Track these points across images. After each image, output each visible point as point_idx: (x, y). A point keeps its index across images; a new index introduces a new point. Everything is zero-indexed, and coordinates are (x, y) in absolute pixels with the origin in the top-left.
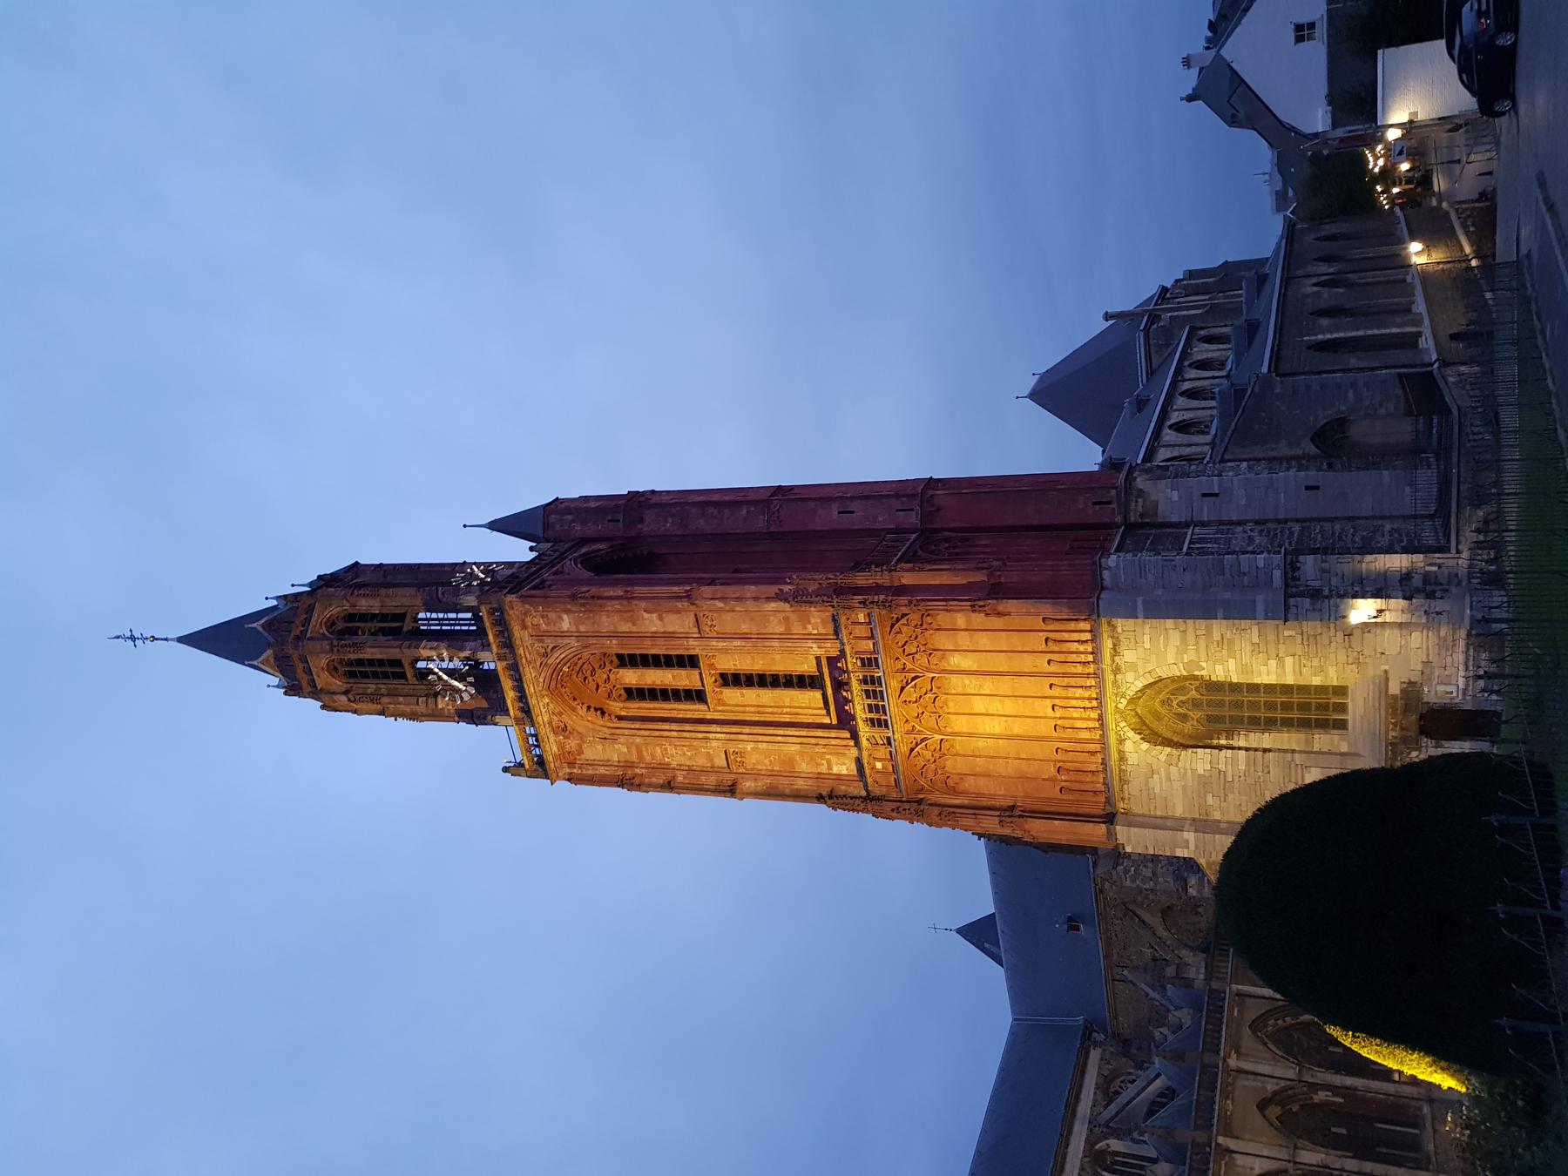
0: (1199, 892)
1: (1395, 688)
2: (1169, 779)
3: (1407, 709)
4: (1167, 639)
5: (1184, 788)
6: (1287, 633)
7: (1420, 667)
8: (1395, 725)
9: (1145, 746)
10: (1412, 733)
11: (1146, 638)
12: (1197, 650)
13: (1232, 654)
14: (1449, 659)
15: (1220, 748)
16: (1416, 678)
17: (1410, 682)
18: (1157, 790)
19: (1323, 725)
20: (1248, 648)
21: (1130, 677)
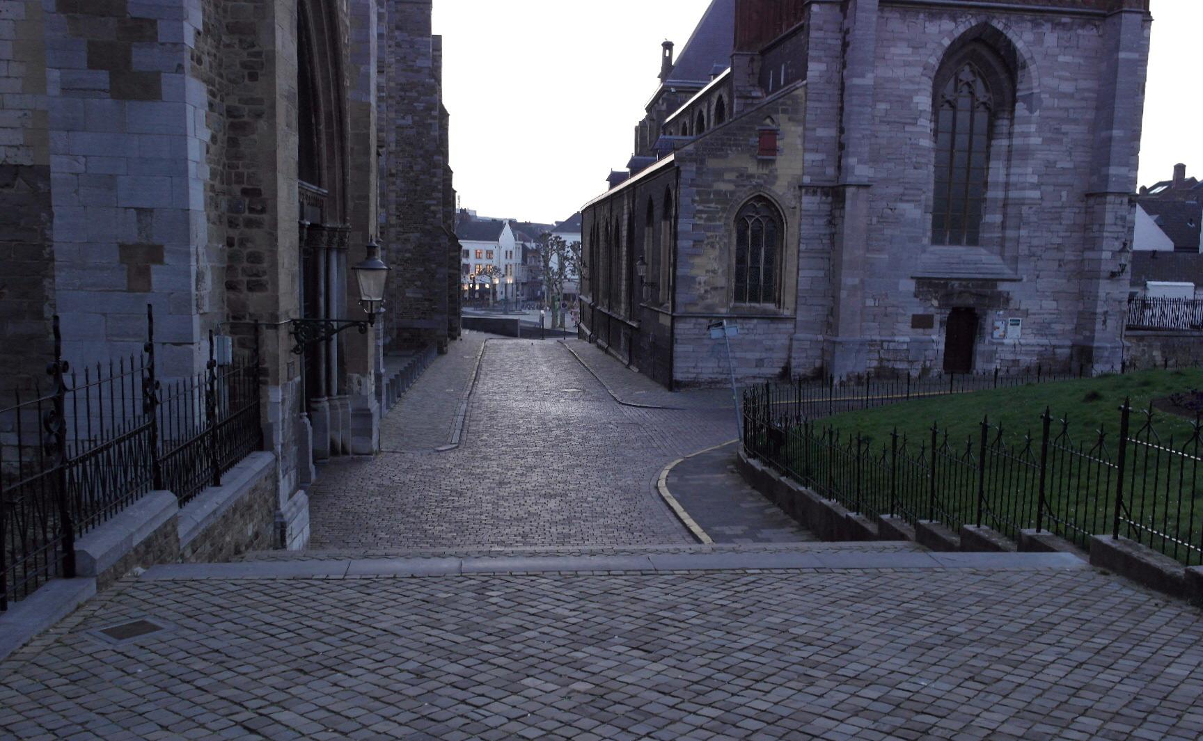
1: (1003, 287)
2: (907, 64)
3: (979, 296)
4: (1067, 79)
5: (896, 80)
6: (1064, 194)
7: (1023, 307)
8: (966, 286)
9: (947, 42)
10: (956, 302)
11: (1068, 59)
13: (1045, 140)
14: (1029, 331)
16: (1012, 305)
17: (1008, 300)
18: (893, 50)
20: (1051, 157)
21: (1028, 36)
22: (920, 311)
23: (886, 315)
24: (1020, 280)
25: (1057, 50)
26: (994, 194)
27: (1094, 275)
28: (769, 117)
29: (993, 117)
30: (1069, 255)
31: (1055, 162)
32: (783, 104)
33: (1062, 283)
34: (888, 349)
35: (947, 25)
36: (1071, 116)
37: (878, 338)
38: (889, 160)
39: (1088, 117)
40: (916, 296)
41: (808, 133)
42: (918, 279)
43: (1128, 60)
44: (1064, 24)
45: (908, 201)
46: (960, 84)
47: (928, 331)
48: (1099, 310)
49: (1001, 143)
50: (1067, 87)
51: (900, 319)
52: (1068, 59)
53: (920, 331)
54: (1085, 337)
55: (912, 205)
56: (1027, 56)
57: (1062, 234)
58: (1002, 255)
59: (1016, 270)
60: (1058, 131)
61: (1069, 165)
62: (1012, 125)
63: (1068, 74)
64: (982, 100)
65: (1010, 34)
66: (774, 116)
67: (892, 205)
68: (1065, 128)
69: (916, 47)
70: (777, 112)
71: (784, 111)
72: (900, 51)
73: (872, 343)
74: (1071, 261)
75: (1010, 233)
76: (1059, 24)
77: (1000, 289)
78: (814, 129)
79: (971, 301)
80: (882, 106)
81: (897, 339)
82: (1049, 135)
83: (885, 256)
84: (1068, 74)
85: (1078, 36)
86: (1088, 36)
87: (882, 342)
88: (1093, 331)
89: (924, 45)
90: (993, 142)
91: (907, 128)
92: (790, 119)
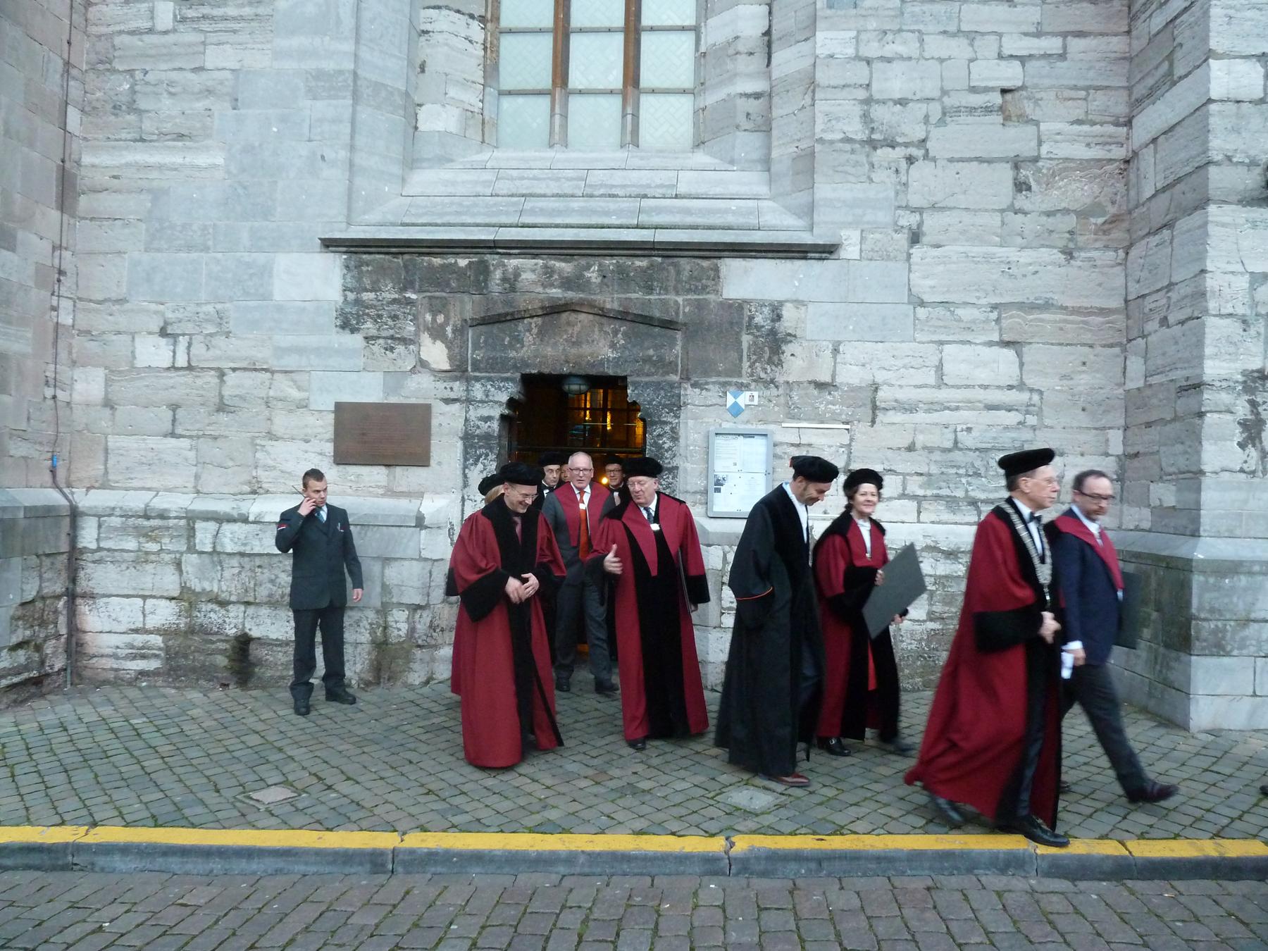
7: (850, 375)
16: (796, 364)
17: (774, 344)
22: (368, 389)
23: (222, 407)
24: (826, 251)
27: (1188, 196)
30: (1063, 135)
33: (1039, 269)
37: (176, 502)
40: (347, 324)
42: (354, 248)
47: (409, 477)
48: (1213, 369)
51: (282, 422)
53: (376, 475)
54: (1161, 512)
57: (1014, 45)
58: (766, 163)
59: (809, 210)
73: (149, 522)
74: (1068, 166)
75: (787, 60)
79: (602, 349)
83: (211, 157)
87: (192, 518)
88: (1193, 477)
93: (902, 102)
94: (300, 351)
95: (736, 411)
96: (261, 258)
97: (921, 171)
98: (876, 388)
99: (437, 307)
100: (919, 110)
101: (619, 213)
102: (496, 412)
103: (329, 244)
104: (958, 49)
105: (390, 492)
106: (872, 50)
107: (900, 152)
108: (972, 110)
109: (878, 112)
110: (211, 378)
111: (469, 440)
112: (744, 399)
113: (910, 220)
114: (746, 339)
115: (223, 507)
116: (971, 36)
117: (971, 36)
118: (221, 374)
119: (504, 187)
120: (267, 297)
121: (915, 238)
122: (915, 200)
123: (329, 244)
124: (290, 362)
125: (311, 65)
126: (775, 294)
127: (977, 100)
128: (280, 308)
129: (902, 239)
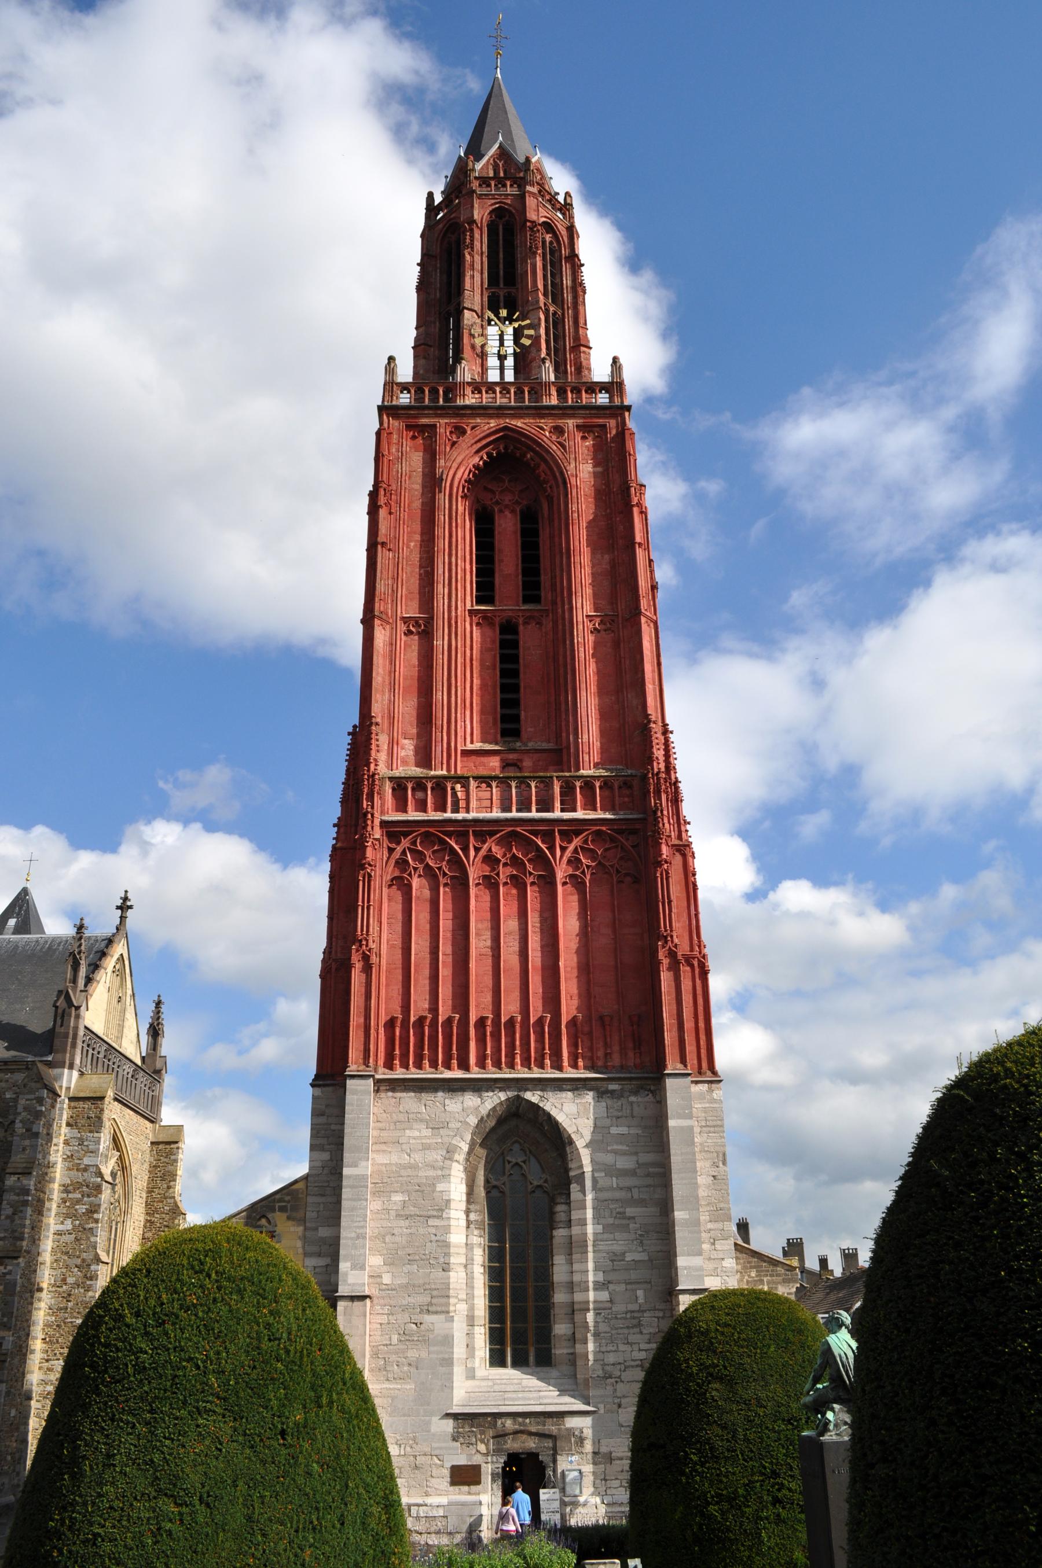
0: (12, 1189)
2: (426, 1147)
5: (414, 1167)
6: (640, 1293)
9: (473, 1121)
10: (513, 1445)
11: (624, 1130)
12: (611, 1189)
14: (617, 1483)
15: (468, 1212)
19: (496, 1337)
20: (617, 1248)
22: (462, 1460)
25: (608, 1122)
26: (559, 1297)
28: (264, 1216)
29: (553, 1202)
31: (624, 1254)
32: (281, 1200)
34: (418, 1518)
35: (470, 1100)
36: (636, 1196)
38: (410, 1262)
39: (657, 1196)
40: (455, 1439)
41: (308, 1234)
43: (682, 1128)
44: (612, 1092)
45: (436, 1313)
46: (508, 1167)
49: (560, 1233)
50: (625, 1163)
52: (624, 1130)
53: (465, 1488)
55: (442, 1317)
56: (570, 1130)
57: (643, 1346)
60: (622, 1215)
61: (643, 1256)
62: (569, 1212)
63: (624, 1148)
64: (536, 1183)
65: (547, 1107)
66: (270, 1216)
67: (416, 1318)
68: (630, 1211)
69: (436, 1128)
70: (274, 1211)
71: (282, 1209)
72: (419, 1133)
76: (607, 1092)
77: (568, 1425)
78: (316, 1229)
79: (531, 1444)
80: (398, 1198)
81: (429, 1500)
82: (611, 1221)
84: (624, 1148)
85: (632, 1103)
86: (640, 1102)
89: (446, 1125)
90: (555, 1233)
91: (431, 1222)
92: (289, 1218)
93: (613, 1364)
94: (440, 1448)
95: (571, 1462)
96: (427, 1418)
97: (620, 1386)
98: (611, 1453)
99: (482, 1433)
100: (618, 1367)
101: (533, 1399)
102: (500, 1466)
103: (448, 1415)
104: (627, 1348)
105: (469, 1493)
106: (604, 1349)
107: (613, 1380)
108: (632, 1367)
109: (608, 1368)
110: (412, 1458)
111: (492, 1474)
112: (573, 1458)
113: (617, 1401)
114: (573, 1440)
115: (420, 1501)
116: (631, 1344)
117: (631, 1344)
118: (415, 1457)
119: (497, 1388)
120: (429, 1431)
121: (619, 1406)
122: (619, 1394)
123: (448, 1415)
124: (437, 1452)
125: (440, 1356)
126: (580, 1425)
127: (633, 1363)
128: (434, 1435)
129: (615, 1406)
